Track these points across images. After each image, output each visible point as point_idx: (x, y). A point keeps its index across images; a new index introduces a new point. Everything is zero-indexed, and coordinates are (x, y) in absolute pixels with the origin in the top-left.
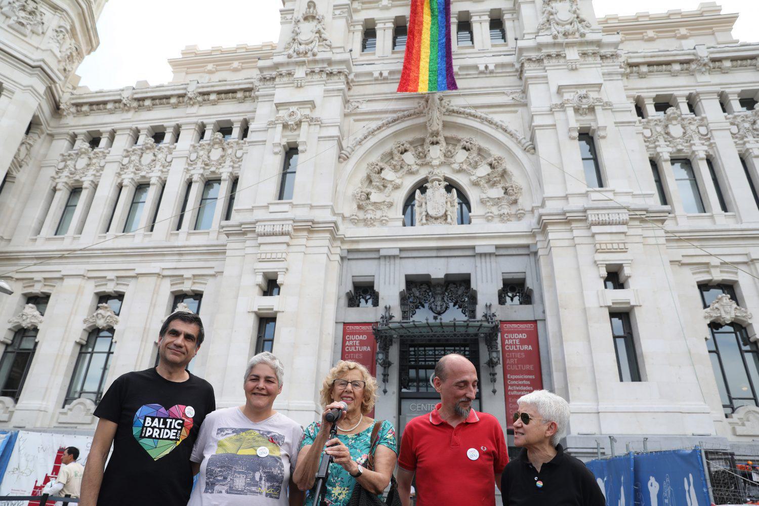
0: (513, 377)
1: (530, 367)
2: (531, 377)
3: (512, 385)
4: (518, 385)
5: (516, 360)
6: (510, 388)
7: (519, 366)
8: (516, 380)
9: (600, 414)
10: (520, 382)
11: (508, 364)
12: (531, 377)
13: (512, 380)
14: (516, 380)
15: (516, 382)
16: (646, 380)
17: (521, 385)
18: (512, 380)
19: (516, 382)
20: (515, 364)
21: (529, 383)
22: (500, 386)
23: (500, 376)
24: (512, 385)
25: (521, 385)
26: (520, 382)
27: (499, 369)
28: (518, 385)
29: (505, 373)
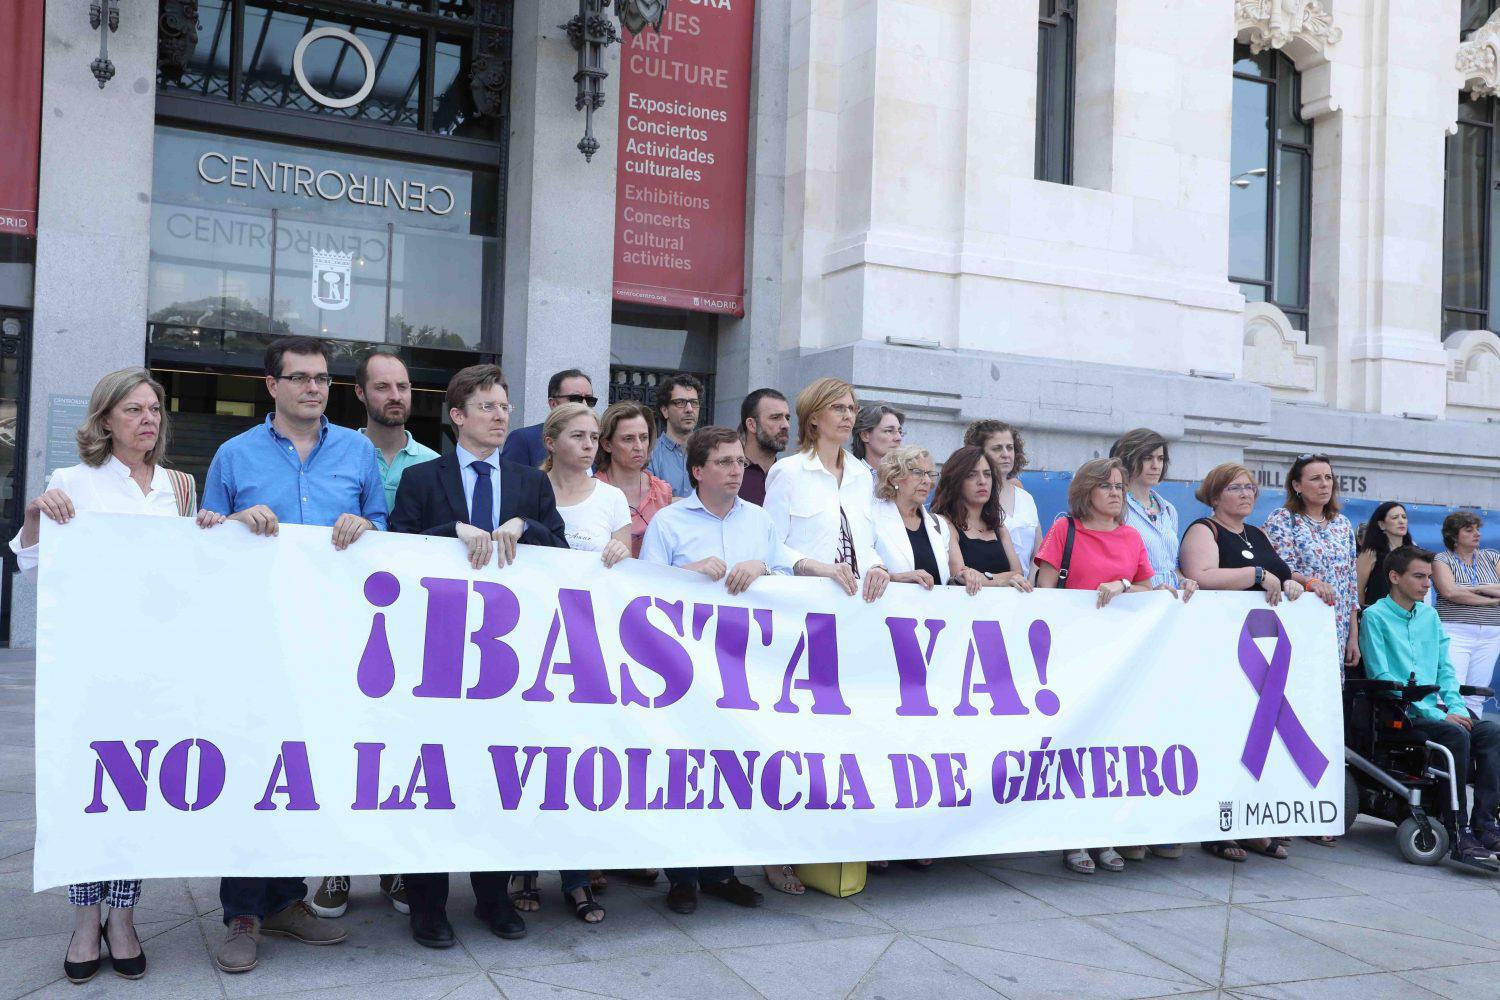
0: (651, 106)
1: (715, 77)
2: (713, 115)
3: (641, 138)
4: (661, 141)
5: (667, 38)
6: (631, 146)
7: (677, 65)
8: (657, 117)
9: (963, 279)
10: (673, 131)
11: (637, 50)
12: (713, 115)
13: (642, 115)
14: (657, 117)
15: (657, 129)
16: (1106, 184)
17: (673, 142)
18: (642, 115)
19: (657, 129)
20: (661, 56)
21: (702, 135)
22: (605, 125)
23: (610, 88)
24: (641, 138)
25: (673, 142)
26: (673, 131)
27: (611, 58)
28: (661, 141)
29: (627, 83)
